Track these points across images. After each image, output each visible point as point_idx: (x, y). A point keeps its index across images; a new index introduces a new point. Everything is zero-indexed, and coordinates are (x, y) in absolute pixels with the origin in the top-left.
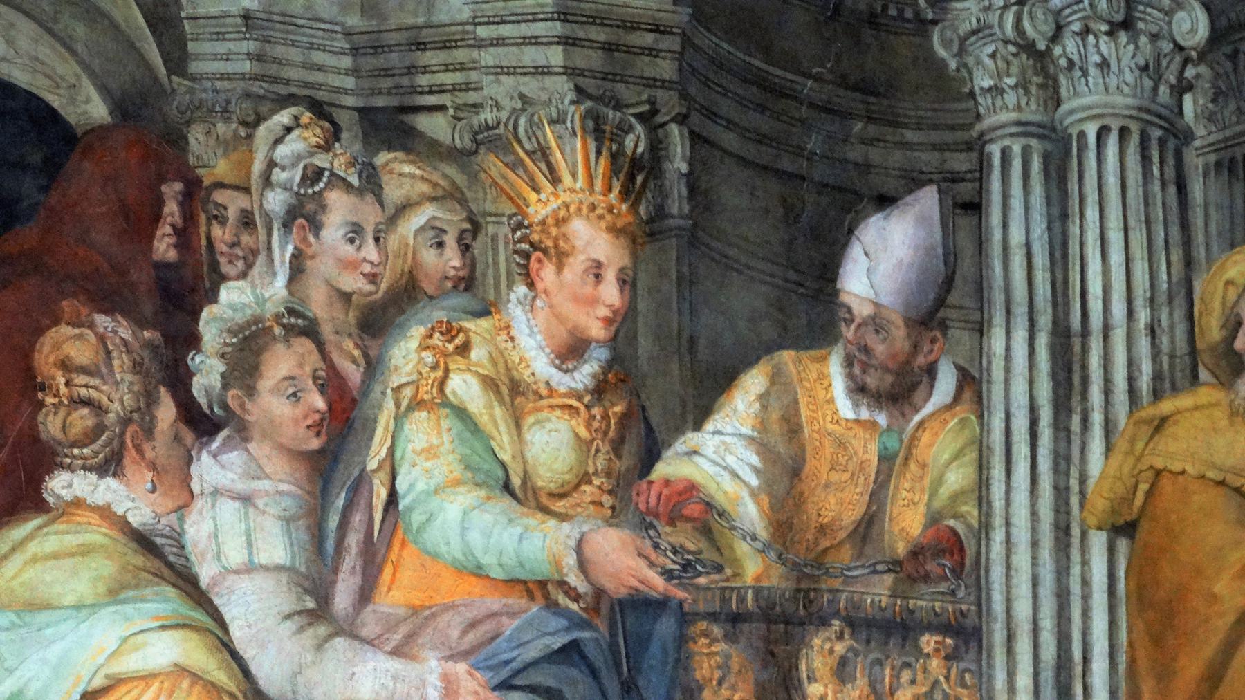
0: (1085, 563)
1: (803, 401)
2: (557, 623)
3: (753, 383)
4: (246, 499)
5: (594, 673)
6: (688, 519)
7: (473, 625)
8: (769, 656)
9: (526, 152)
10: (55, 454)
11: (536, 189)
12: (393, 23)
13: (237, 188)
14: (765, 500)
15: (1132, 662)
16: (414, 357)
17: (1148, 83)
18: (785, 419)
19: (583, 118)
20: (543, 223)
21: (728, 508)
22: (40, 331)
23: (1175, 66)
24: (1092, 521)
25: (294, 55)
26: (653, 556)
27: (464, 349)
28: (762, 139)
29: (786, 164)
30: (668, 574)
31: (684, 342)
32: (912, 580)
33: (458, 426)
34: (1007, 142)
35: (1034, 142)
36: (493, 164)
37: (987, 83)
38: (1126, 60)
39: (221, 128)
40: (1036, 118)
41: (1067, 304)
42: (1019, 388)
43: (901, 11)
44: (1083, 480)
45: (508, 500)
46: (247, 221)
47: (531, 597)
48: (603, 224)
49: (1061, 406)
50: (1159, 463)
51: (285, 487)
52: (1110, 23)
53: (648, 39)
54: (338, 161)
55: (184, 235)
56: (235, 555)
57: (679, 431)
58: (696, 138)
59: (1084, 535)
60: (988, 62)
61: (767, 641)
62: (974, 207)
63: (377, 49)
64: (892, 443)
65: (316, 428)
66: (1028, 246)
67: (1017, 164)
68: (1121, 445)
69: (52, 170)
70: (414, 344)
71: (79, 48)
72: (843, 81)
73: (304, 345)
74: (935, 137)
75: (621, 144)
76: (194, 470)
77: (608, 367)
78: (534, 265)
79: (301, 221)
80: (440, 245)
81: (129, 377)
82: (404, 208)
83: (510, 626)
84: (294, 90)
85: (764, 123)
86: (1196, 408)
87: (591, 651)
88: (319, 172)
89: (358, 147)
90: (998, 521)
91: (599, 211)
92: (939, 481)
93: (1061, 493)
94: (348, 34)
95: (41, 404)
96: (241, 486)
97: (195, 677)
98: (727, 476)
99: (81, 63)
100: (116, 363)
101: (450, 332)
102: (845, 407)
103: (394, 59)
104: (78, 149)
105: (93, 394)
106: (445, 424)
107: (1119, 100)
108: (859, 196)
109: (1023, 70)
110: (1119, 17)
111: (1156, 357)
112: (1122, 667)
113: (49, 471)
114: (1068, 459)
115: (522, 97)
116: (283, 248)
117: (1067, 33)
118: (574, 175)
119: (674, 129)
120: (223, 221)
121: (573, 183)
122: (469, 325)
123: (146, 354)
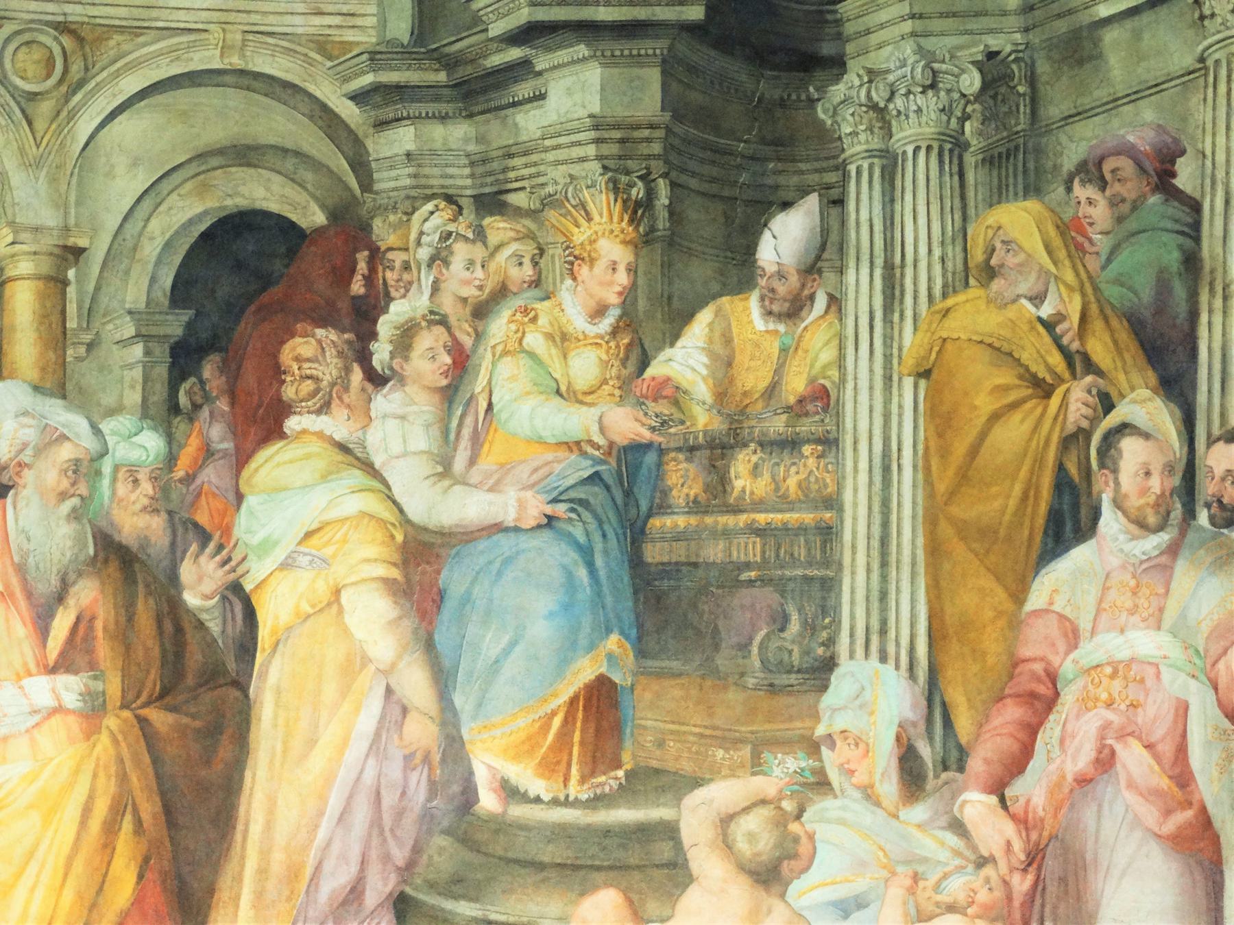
0: (900, 395)
1: (734, 324)
3: (705, 317)
4: (403, 418)
5: (608, 488)
6: (665, 397)
7: (536, 470)
9: (574, 207)
10: (290, 406)
11: (578, 226)
12: (495, 145)
13: (400, 249)
14: (711, 381)
15: (927, 449)
16: (504, 328)
17: (945, 118)
18: (724, 335)
19: (607, 183)
20: (582, 244)
21: (688, 388)
22: (283, 342)
23: (961, 107)
24: (905, 371)
25: (436, 171)
26: (644, 419)
27: (534, 320)
28: (713, 180)
29: (726, 193)
30: (653, 429)
31: (665, 299)
33: (531, 362)
34: (860, 163)
35: (876, 161)
36: (552, 215)
37: (848, 130)
38: (932, 106)
39: (392, 218)
40: (876, 147)
41: (893, 251)
43: (799, 97)
44: (900, 349)
45: (559, 398)
46: (406, 267)
47: (571, 451)
48: (618, 240)
49: (888, 309)
50: (945, 335)
51: (425, 408)
52: (923, 86)
53: (646, 133)
54: (462, 227)
55: (369, 280)
56: (396, 448)
57: (660, 349)
58: (674, 185)
59: (900, 379)
60: (850, 118)
61: (711, 459)
62: (840, 202)
64: (788, 340)
65: (445, 374)
66: (871, 220)
68: (923, 326)
69: (292, 254)
70: (505, 320)
71: (309, 186)
72: (763, 141)
73: (439, 330)
74: (817, 165)
75: (629, 194)
76: (372, 405)
77: (621, 317)
78: (576, 268)
79: (438, 262)
80: (521, 264)
81: (335, 360)
82: (498, 248)
83: (558, 468)
84: (435, 191)
85: (715, 171)
86: (967, 301)
87: (606, 476)
88: (450, 234)
89: (473, 216)
90: (850, 377)
91: (616, 233)
92: (816, 359)
93: (888, 358)
94: (468, 156)
95: (284, 381)
96: (400, 412)
97: (372, 517)
98: (689, 371)
100: (328, 354)
101: (526, 311)
102: (759, 323)
103: (495, 165)
104: (307, 241)
105: (314, 372)
106: (522, 362)
107: (928, 130)
108: (771, 204)
109: (870, 121)
110: (929, 82)
111: (944, 275)
112: (921, 452)
113: (287, 417)
114: (892, 338)
115: (571, 176)
116: (427, 278)
117: (897, 95)
118: (601, 215)
119: (661, 181)
120: (392, 269)
121: (600, 220)
122: (538, 306)
123: (346, 347)
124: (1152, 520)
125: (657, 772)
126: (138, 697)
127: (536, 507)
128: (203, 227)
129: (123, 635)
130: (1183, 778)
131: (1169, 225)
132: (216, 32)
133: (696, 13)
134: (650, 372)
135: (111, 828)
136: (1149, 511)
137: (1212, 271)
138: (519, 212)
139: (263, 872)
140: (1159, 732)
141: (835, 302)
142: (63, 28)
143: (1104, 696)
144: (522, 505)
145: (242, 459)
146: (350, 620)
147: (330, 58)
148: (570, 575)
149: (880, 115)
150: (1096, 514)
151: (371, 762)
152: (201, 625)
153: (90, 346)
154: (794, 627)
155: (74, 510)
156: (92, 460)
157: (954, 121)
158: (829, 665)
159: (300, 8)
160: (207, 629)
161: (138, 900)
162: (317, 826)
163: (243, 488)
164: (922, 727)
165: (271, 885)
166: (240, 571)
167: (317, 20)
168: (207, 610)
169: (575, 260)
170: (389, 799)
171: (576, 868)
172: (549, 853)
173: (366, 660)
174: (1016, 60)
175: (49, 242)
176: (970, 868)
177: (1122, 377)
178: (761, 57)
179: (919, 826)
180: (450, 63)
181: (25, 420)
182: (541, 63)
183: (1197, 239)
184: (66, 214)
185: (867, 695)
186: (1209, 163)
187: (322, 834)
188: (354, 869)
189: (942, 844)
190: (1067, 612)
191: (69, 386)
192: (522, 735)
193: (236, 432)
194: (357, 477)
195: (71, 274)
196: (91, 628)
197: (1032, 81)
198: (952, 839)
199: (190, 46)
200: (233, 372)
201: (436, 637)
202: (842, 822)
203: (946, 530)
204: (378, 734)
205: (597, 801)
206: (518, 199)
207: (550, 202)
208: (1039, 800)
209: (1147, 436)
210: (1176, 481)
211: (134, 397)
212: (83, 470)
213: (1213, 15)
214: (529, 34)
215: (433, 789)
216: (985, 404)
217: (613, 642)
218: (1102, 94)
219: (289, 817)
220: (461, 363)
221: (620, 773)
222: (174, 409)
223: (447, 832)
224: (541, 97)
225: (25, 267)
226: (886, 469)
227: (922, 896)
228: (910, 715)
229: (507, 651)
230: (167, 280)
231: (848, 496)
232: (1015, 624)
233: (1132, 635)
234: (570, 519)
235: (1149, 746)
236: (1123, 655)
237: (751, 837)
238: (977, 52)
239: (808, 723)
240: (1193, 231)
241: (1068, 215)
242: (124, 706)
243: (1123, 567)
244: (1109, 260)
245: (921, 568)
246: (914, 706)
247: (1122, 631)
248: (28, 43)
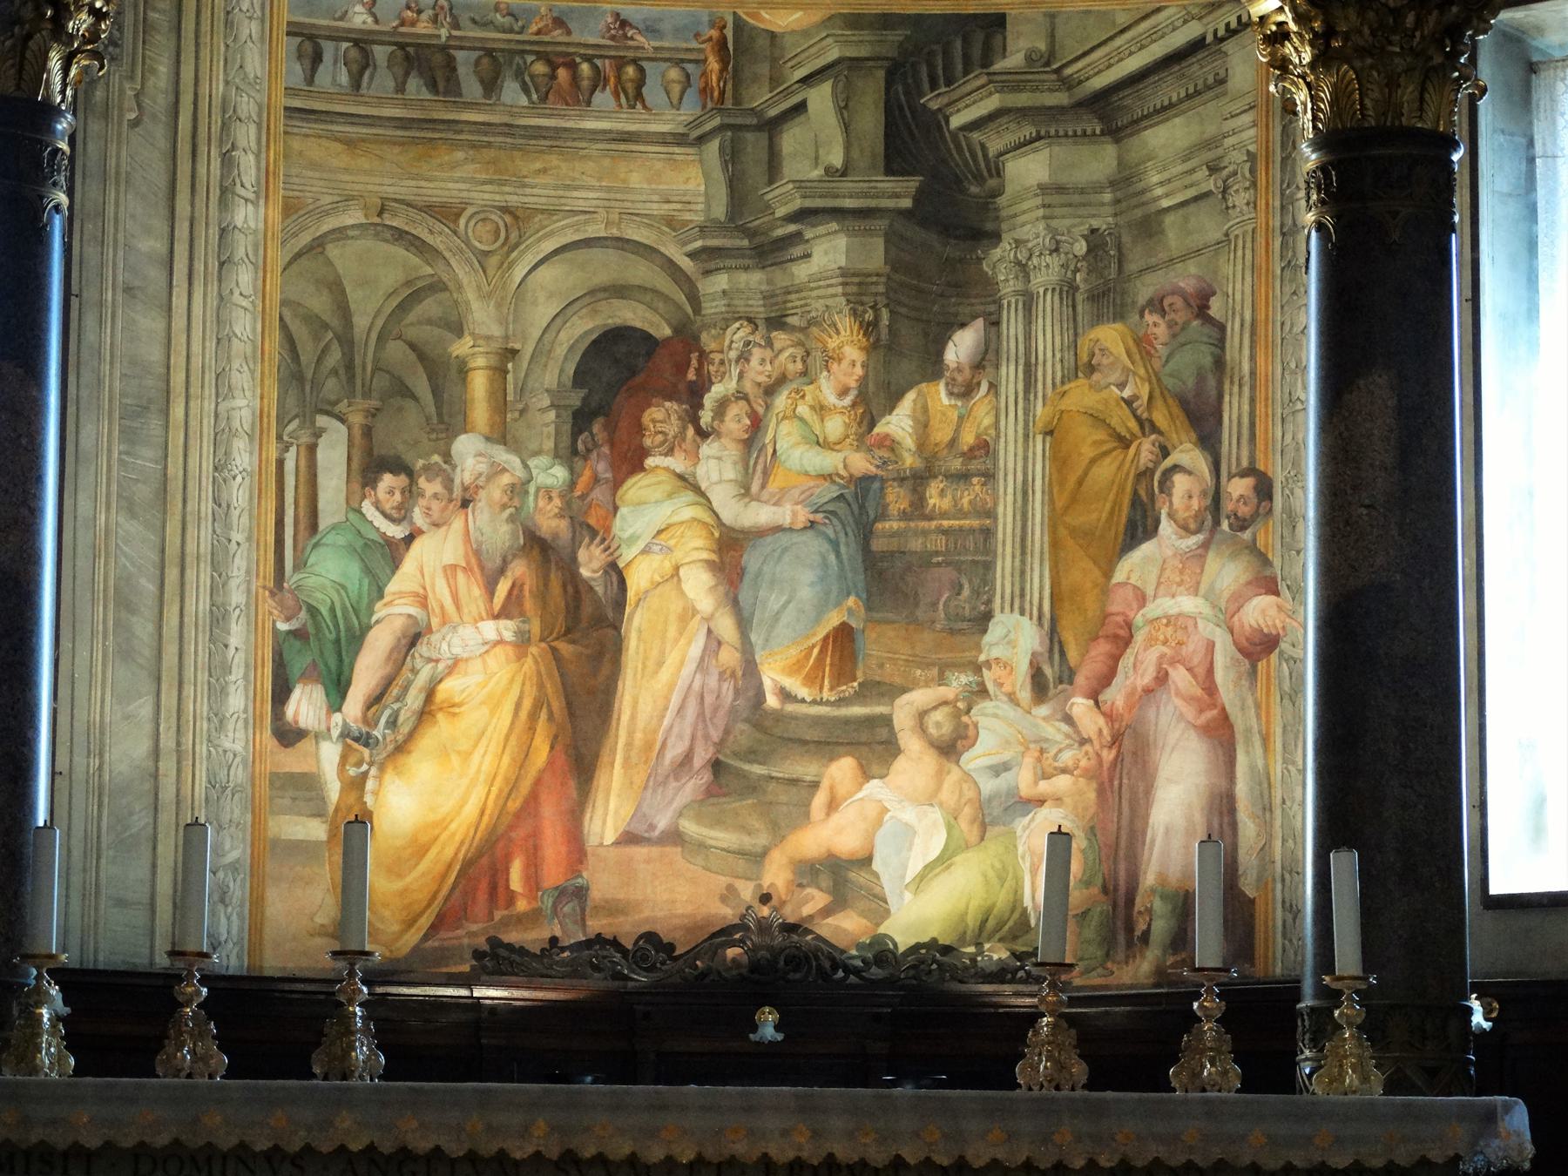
0: (1034, 446)
2: (835, 488)
3: (910, 396)
4: (719, 458)
5: (849, 505)
7: (803, 492)
8: (914, 490)
25: (742, 303)
27: (803, 397)
29: (925, 317)
30: (878, 467)
32: (970, 459)
36: (815, 330)
39: (713, 331)
42: (1011, 386)
44: (1034, 416)
49: (1027, 391)
50: (1063, 408)
54: (758, 338)
55: (699, 371)
56: (715, 477)
57: (883, 415)
62: (997, 323)
63: (772, 296)
64: (963, 411)
67: (1013, 306)
68: (1049, 402)
72: (949, 284)
73: (742, 403)
77: (857, 397)
82: (781, 351)
90: (1002, 435)
92: (980, 424)
96: (719, 454)
99: (661, 316)
101: (797, 392)
102: (945, 400)
103: (779, 299)
111: (1063, 368)
121: (845, 334)
122: (806, 388)
124: (1193, 526)
125: (879, 683)
126: (551, 634)
127: (803, 515)
128: (594, 337)
129: (542, 595)
130: (1210, 688)
131: (1205, 339)
132: (602, 213)
133: (906, 203)
134: (876, 430)
135: (533, 717)
136: (1191, 520)
137: (1232, 369)
138: (793, 329)
139: (629, 745)
140: (1196, 661)
141: (994, 387)
142: (505, 210)
143: (1161, 637)
144: (794, 514)
145: (617, 484)
146: (686, 587)
147: (674, 230)
148: (824, 558)
149: (1023, 269)
150: (1157, 522)
151: (698, 676)
152: (591, 588)
153: (522, 412)
154: (966, 592)
155: (511, 515)
156: (523, 484)
157: (1069, 273)
158: (987, 617)
159: (655, 198)
160: (595, 593)
161: (551, 762)
162: (663, 717)
163: (618, 502)
164: (1047, 655)
165: (633, 754)
166: (616, 554)
167: (666, 206)
168: (594, 579)
169: (830, 359)
170: (709, 700)
171: (829, 743)
172: (810, 735)
173: (695, 612)
174: (1110, 234)
175: (495, 346)
176: (1076, 745)
177: (1174, 436)
178: (948, 230)
179: (1045, 719)
180: (751, 234)
181: (480, 459)
182: (808, 234)
183: (1223, 348)
184: (507, 329)
185: (1012, 636)
186: (1230, 301)
187: (666, 722)
188: (687, 743)
189: (1059, 730)
190: (1139, 584)
191: (508, 437)
192: (795, 660)
193: (614, 467)
194: (690, 496)
195: (510, 366)
196: (521, 590)
197: (1119, 248)
198: (1065, 727)
199: (586, 222)
200: (611, 428)
201: (740, 597)
202: (996, 716)
203: (1063, 532)
204: (702, 659)
205: (842, 702)
206: (793, 320)
207: (812, 322)
208: (1120, 703)
209: (1190, 473)
210: (1209, 501)
211: (549, 444)
212: (517, 490)
213: (1234, 207)
214: (801, 215)
215: (737, 692)
216: (1088, 452)
217: (851, 601)
218: (1163, 256)
219: (646, 709)
220: (757, 424)
221: (855, 684)
222: (575, 452)
223: (747, 720)
224: (808, 256)
225: (480, 361)
226: (1025, 493)
227: (1048, 761)
228: (1039, 649)
229: (784, 606)
230: (571, 369)
231: (1000, 509)
232: (1105, 591)
233: (1179, 599)
234: (825, 524)
235: (1189, 670)
236: (1173, 611)
237: (938, 725)
238: (1084, 229)
239: (974, 653)
240: (1221, 343)
241: (1141, 334)
242: (542, 640)
243: (1175, 555)
244: (1167, 361)
245: (1047, 556)
246: (1041, 643)
247: (1173, 596)
248: (483, 220)
